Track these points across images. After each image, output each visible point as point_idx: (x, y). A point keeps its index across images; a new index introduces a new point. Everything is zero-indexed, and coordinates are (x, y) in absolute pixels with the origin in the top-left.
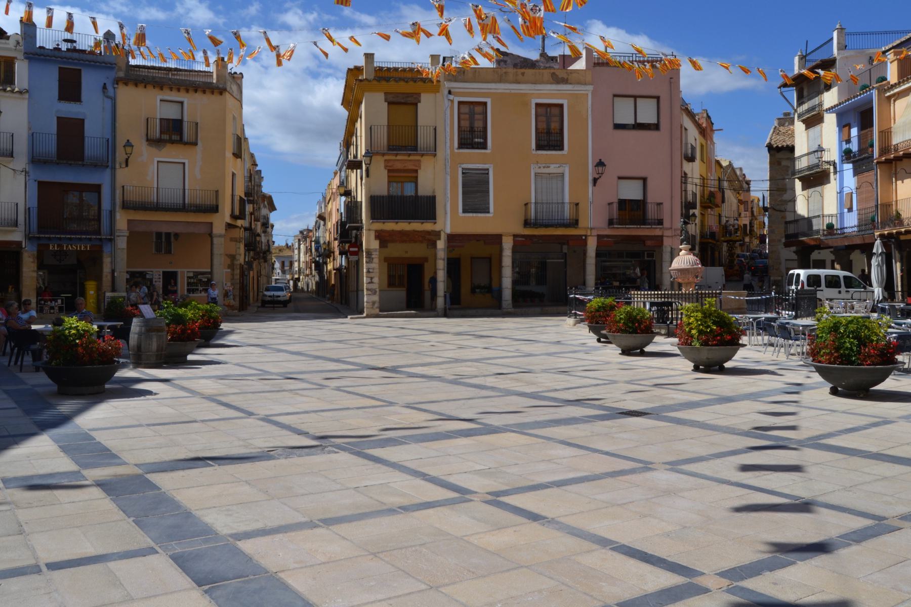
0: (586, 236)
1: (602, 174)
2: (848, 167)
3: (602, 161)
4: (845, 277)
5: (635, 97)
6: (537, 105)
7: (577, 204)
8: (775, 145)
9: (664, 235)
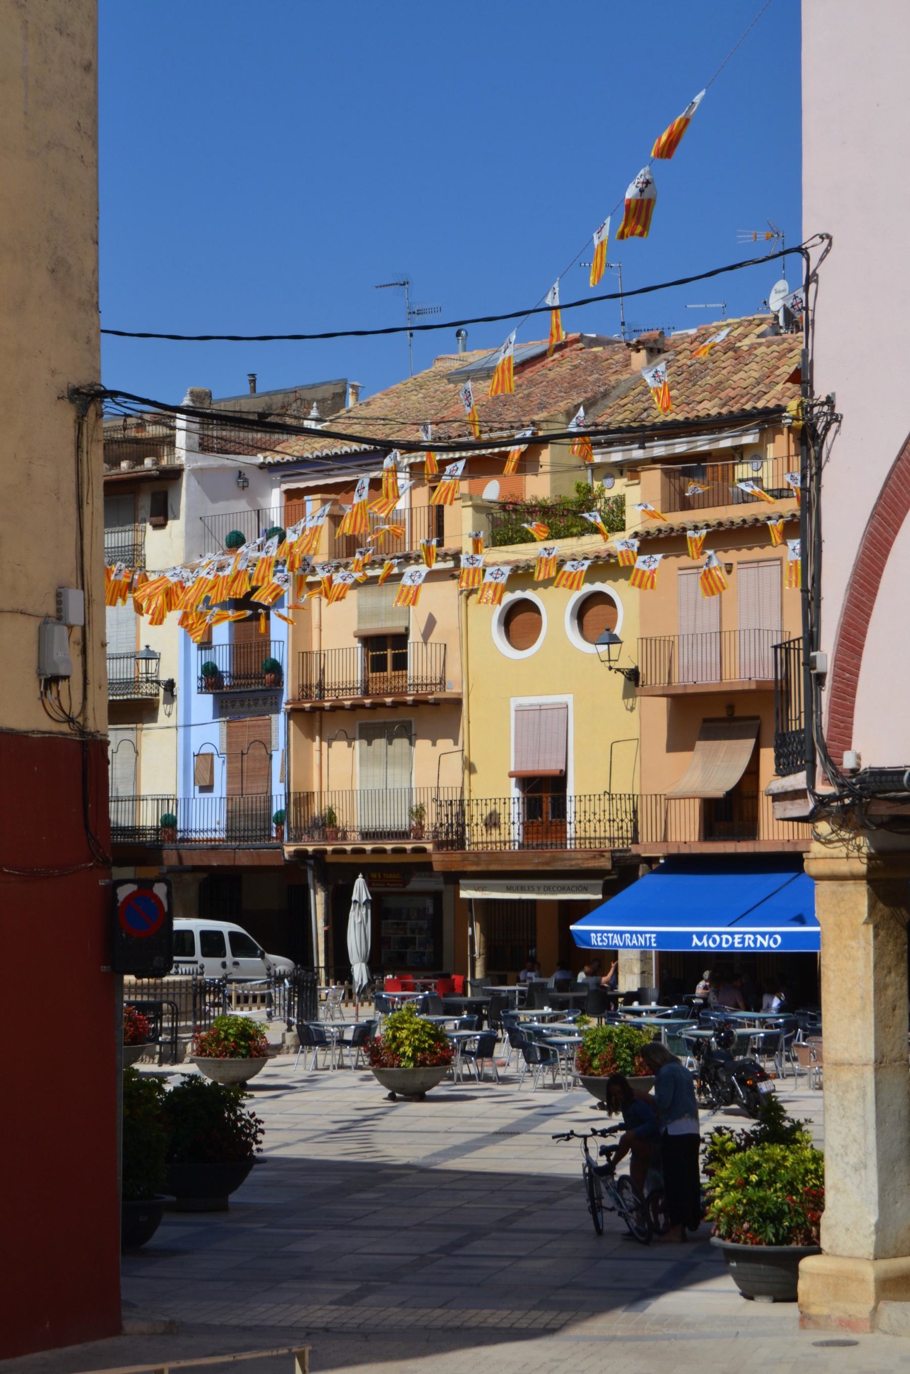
2: (204, 704)
4: (232, 934)
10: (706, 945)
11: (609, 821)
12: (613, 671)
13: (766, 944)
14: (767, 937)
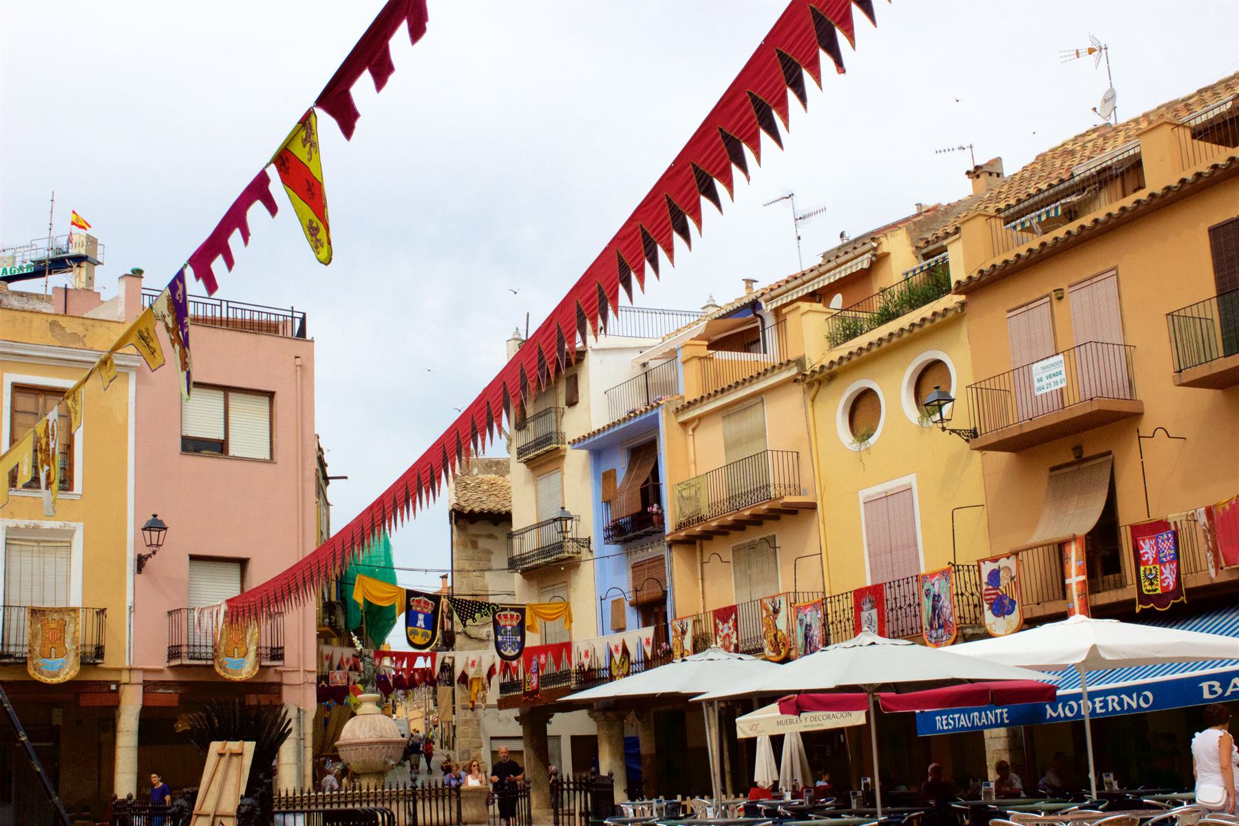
0: (118, 684)
1: (158, 545)
3: (159, 518)
5: (227, 390)
6: (18, 388)
7: (102, 612)
8: (469, 509)
9: (285, 681)
10: (1062, 715)
11: (957, 594)
12: (947, 432)
13: (1134, 705)
14: (1135, 695)
